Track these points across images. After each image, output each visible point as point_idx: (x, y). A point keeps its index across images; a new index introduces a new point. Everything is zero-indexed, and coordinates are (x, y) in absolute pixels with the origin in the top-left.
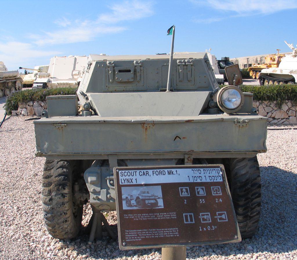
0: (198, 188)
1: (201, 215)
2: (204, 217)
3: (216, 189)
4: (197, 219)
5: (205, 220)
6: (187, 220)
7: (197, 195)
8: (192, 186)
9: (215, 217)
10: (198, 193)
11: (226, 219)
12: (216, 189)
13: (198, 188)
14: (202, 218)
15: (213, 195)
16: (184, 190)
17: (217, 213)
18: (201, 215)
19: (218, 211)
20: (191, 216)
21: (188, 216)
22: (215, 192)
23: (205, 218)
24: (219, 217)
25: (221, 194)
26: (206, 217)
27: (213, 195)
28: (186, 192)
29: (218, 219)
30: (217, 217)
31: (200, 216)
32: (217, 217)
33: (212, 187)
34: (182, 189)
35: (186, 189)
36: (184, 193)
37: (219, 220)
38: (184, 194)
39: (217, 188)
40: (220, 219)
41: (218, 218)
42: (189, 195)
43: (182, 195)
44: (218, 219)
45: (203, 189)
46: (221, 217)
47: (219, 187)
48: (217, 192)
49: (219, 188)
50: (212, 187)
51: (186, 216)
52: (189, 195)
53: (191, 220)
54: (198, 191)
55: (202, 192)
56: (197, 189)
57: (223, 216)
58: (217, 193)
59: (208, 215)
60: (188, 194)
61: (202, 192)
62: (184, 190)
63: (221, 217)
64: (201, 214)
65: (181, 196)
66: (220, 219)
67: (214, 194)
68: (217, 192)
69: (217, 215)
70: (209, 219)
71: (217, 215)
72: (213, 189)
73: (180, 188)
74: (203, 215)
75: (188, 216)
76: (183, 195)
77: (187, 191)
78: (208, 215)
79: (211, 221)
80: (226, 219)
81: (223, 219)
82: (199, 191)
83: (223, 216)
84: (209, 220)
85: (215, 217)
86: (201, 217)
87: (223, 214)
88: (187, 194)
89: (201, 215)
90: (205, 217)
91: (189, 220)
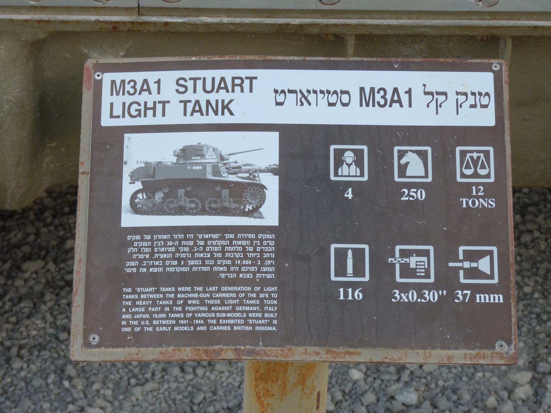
0: (406, 151)
1: (397, 254)
3: (475, 155)
4: (382, 269)
6: (341, 270)
8: (381, 141)
9: (450, 264)
10: (403, 169)
11: (492, 277)
12: (475, 155)
13: (406, 151)
14: (401, 265)
15: (459, 179)
16: (349, 157)
17: (461, 249)
18: (397, 254)
20: (358, 255)
21: (350, 253)
22: (468, 167)
23: (413, 266)
24: (467, 265)
25: (492, 180)
27: (459, 179)
28: (353, 167)
29: (461, 272)
30: (460, 265)
31: (393, 256)
32: (460, 265)
33: (458, 149)
34: (339, 154)
35: (358, 154)
36: (345, 166)
38: (346, 173)
39: (478, 152)
40: (473, 273)
41: (462, 268)
42: (366, 178)
43: (336, 174)
44: (461, 272)
45: (422, 155)
46: (474, 265)
47: (491, 149)
48: (476, 168)
49: (487, 154)
50: (458, 149)
51: (341, 255)
52: (366, 178)
53: (359, 271)
54: (403, 161)
55: (415, 166)
56: (402, 154)
57: (484, 265)
58: (476, 175)
59: (426, 253)
60: (362, 175)
61: (415, 166)
62: (349, 157)
63: (474, 265)
64: (398, 248)
65: (333, 178)
67: (463, 176)
69: (461, 257)
70: (427, 271)
71: (461, 257)
72: (463, 154)
74: (405, 254)
75: (350, 253)
76: (342, 176)
77: (359, 163)
78: (426, 253)
80: (492, 277)
81: (484, 276)
82: (407, 164)
83: (484, 265)
84: (428, 276)
85: (450, 264)
86: (397, 261)
87: (483, 254)
88: (358, 174)
89: (401, 250)
90: (413, 261)
91: (350, 269)
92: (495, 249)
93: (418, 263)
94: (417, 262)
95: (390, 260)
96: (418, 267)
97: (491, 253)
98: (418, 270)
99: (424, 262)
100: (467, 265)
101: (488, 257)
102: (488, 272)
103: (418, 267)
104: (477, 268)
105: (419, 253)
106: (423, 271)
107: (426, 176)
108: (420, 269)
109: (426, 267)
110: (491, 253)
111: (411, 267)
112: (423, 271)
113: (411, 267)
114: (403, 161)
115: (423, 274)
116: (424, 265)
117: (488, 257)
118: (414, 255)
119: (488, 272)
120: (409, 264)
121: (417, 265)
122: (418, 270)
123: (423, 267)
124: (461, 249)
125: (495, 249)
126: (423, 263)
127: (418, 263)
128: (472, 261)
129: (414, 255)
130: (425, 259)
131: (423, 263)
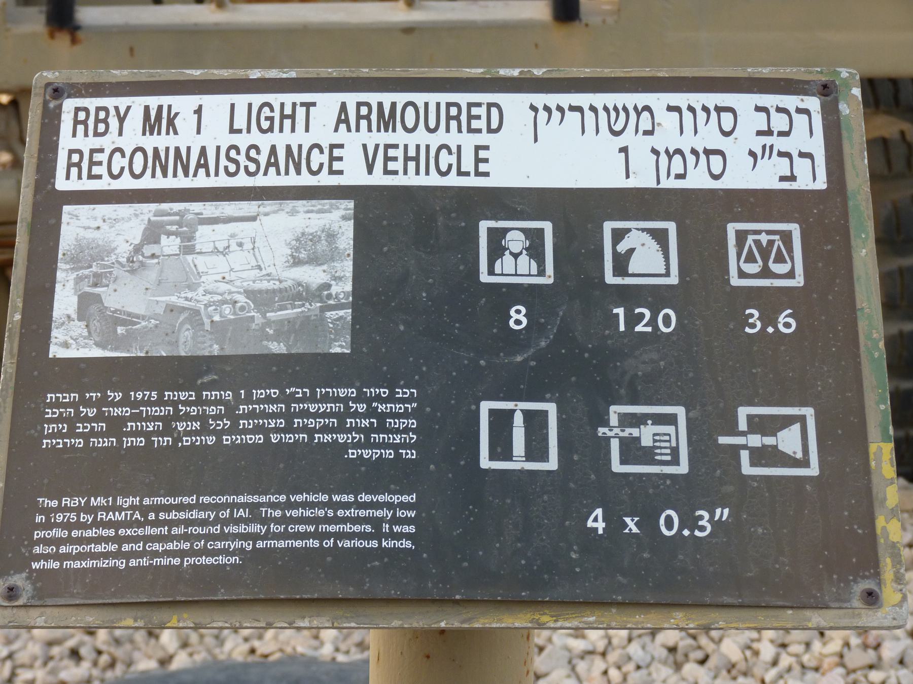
2: (635, 432)
5: (647, 456)
7: (610, 278)
9: (723, 440)
13: (628, 230)
17: (743, 412)
19: (751, 404)
23: (646, 442)
24: (755, 440)
26: (657, 435)
29: (745, 455)
37: (753, 464)
41: (745, 447)
44: (745, 455)
46: (769, 441)
54: (622, 248)
57: (788, 441)
59: (671, 420)
63: (769, 441)
66: (761, 456)
68: (765, 260)
69: (743, 426)
70: (675, 452)
71: (743, 426)
73: (484, 226)
78: (671, 420)
79: (683, 468)
83: (788, 441)
84: (675, 461)
90: (646, 435)
92: (809, 412)
93: (657, 438)
94: (654, 435)
95: (601, 431)
96: (657, 444)
97: (802, 419)
98: (658, 451)
99: (669, 435)
100: (755, 440)
101: (796, 427)
102: (799, 455)
103: (657, 444)
104: (775, 447)
105: (660, 419)
106: (668, 451)
107: (667, 274)
108: (661, 448)
109: (674, 444)
110: (802, 419)
111: (643, 444)
112: (668, 451)
113: (643, 444)
114: (622, 248)
115: (669, 458)
116: (669, 441)
117: (796, 427)
118: (650, 422)
119: (799, 455)
120: (638, 439)
121: (655, 441)
122: (658, 451)
123: (667, 444)
124: (743, 412)
125: (809, 412)
126: (667, 438)
127: (657, 438)
128: (764, 434)
129: (650, 422)
130: (670, 429)
131: (667, 438)
